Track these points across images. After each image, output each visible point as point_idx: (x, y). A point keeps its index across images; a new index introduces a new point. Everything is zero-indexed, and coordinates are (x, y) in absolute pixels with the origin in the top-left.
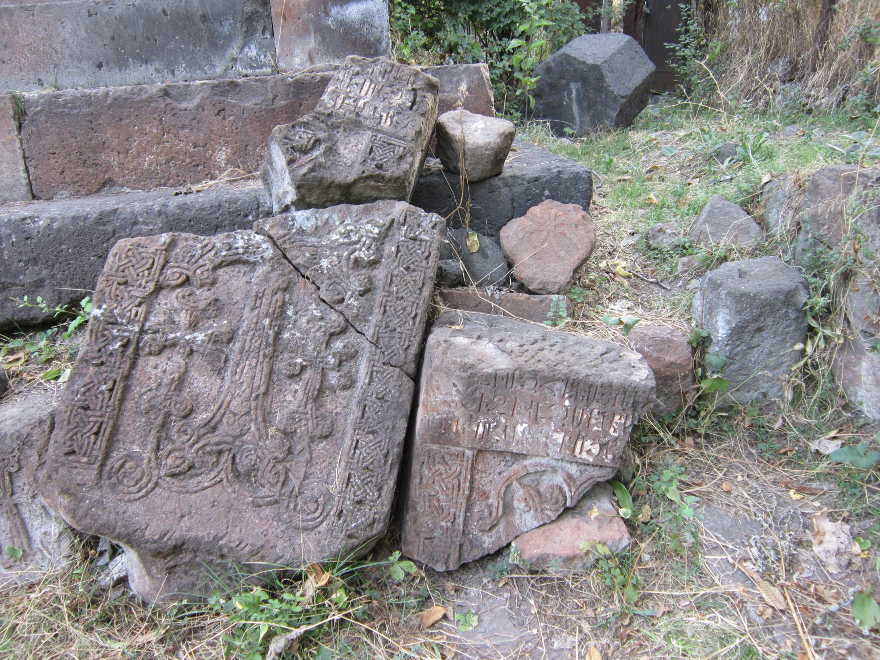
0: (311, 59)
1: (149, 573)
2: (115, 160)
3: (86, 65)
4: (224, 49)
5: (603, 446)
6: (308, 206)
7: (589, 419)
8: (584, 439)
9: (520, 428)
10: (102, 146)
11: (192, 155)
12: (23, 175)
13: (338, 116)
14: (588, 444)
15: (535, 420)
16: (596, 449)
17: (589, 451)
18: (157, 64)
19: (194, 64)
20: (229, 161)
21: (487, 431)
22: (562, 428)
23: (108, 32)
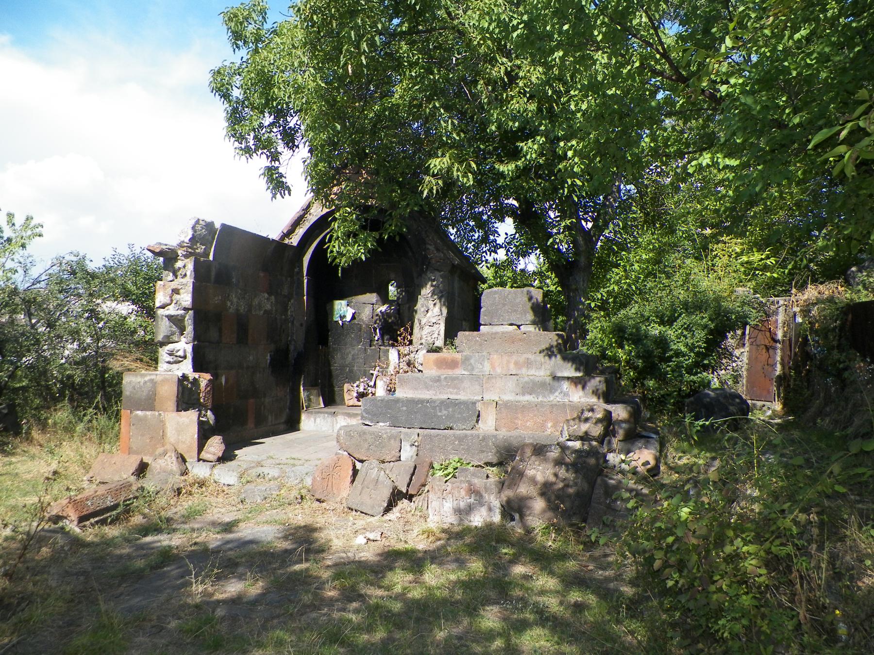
2: (520, 422)
3: (513, 394)
10: (517, 418)
19: (544, 396)
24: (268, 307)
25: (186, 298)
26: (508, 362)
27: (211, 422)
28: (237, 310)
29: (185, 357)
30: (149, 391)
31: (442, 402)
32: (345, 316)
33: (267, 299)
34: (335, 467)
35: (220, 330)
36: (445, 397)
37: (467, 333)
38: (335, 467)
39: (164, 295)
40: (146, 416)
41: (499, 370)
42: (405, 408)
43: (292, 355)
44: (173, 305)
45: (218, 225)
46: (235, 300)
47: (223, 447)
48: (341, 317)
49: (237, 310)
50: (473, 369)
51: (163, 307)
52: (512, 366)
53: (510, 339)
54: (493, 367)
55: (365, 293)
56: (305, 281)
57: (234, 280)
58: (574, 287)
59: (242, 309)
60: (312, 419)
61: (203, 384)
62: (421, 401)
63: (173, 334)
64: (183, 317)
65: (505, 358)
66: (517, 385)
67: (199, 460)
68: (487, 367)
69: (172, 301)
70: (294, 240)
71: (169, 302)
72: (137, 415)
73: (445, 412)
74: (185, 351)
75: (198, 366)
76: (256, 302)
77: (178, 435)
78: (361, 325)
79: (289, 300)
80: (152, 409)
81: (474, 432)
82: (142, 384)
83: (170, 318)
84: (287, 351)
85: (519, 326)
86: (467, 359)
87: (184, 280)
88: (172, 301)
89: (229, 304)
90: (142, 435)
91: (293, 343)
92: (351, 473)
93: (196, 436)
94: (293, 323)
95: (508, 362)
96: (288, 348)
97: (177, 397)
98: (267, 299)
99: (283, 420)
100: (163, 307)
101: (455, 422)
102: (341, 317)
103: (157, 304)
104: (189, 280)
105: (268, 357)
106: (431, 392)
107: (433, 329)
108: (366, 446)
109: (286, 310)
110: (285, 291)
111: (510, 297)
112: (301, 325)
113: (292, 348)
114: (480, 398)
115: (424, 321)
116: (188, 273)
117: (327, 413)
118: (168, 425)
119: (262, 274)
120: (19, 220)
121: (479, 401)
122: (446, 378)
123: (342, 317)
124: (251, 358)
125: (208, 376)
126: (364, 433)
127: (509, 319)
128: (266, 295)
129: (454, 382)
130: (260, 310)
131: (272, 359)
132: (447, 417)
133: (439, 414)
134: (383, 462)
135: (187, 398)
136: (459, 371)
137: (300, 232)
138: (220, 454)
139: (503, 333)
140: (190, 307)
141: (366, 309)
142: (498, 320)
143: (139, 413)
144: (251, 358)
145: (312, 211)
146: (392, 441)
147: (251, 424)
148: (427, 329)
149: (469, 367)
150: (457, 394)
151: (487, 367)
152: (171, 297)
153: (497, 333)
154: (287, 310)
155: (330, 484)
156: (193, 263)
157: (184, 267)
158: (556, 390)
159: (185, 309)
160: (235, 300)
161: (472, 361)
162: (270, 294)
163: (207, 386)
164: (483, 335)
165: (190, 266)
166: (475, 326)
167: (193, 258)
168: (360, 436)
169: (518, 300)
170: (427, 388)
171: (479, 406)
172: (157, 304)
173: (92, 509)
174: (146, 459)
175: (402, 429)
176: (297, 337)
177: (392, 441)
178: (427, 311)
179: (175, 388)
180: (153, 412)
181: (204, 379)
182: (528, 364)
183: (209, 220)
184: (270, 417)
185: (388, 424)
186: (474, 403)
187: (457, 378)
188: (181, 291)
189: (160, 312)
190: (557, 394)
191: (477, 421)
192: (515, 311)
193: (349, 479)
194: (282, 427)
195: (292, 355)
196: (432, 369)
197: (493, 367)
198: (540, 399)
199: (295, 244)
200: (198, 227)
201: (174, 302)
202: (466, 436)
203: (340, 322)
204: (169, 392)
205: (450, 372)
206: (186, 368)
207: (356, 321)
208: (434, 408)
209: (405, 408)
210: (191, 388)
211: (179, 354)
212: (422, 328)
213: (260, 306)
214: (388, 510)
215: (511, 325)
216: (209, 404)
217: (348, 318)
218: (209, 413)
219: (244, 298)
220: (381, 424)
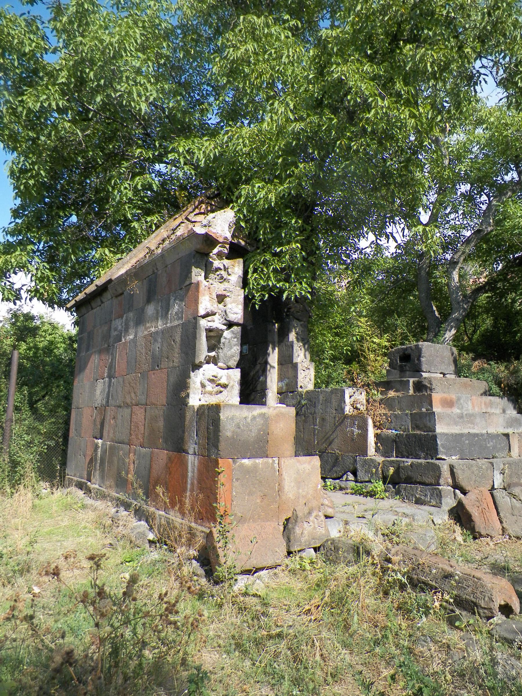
30: (259, 430)
36: (466, 431)
40: (255, 466)
51: (207, 315)
52: (483, 406)
54: (473, 407)
62: (462, 435)
72: (242, 465)
77: (299, 488)
82: (249, 420)
83: (209, 330)
86: (459, 399)
90: (250, 494)
101: (498, 452)
103: (202, 312)
106: (458, 427)
118: (285, 475)
126: (472, 466)
143: (246, 462)
161: (462, 401)
170: (456, 423)
179: (294, 426)
180: (265, 460)
185: (458, 457)
211: (223, 381)
220: (454, 457)
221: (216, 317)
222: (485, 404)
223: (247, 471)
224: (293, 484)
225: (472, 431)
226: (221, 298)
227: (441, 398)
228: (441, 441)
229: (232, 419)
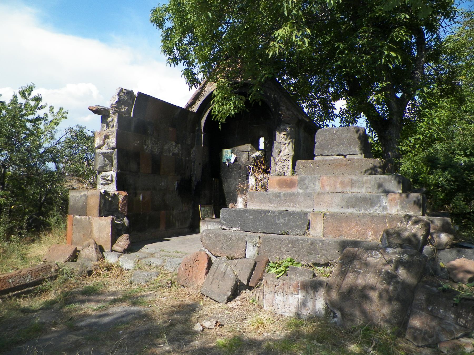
0: (398, 211)
1: (343, 320)
2: (344, 230)
3: (339, 207)
4: (374, 206)
5: (466, 322)
6: (391, 248)
7: (462, 313)
8: (460, 318)
9: (441, 311)
10: (341, 227)
11: (363, 232)
12: (322, 230)
13: (401, 228)
14: (461, 319)
15: (445, 310)
16: (464, 322)
17: (462, 322)
18: (356, 209)
19: (365, 209)
20: (372, 235)
21: (432, 309)
22: (454, 314)
23: (346, 200)
24: (176, 151)
25: (113, 141)
26: (335, 182)
27: (126, 225)
28: (152, 151)
29: (112, 181)
30: (84, 202)
31: (280, 212)
32: (230, 160)
33: (175, 146)
34: (195, 260)
35: (139, 164)
36: (283, 209)
37: (303, 161)
38: (195, 260)
39: (100, 140)
40: (81, 219)
41: (327, 189)
42: (251, 217)
43: (194, 184)
44: (105, 146)
45: (136, 93)
46: (150, 145)
47: (128, 242)
48: (227, 160)
49: (152, 151)
50: (307, 188)
51: (99, 147)
52: (338, 185)
53: (338, 165)
54: (323, 186)
55: (244, 144)
56: (203, 135)
57: (149, 131)
58: (389, 138)
59: (156, 151)
60: (206, 226)
61: (121, 198)
62: (264, 212)
63: (106, 165)
64: (112, 153)
65: (333, 179)
66: (343, 199)
67: (112, 251)
68: (318, 186)
69: (104, 143)
70: (195, 109)
71: (102, 144)
73: (282, 221)
74: (112, 177)
75: (119, 188)
76: (166, 147)
78: (241, 166)
79: (192, 148)
80: (85, 215)
81: (305, 237)
82: (79, 197)
83: (104, 154)
84: (190, 180)
85: (345, 156)
86: (302, 180)
87: (112, 130)
88: (104, 143)
89: (145, 147)
91: (194, 176)
92: (206, 266)
93: (110, 234)
94: (194, 162)
95: (335, 182)
96: (191, 178)
97: (100, 206)
98: (175, 146)
99: (187, 226)
100: (99, 147)
101: (290, 229)
102: (227, 160)
103: (96, 146)
104: (115, 129)
105: (176, 184)
106: (273, 205)
107: (284, 164)
108: (220, 245)
109: (189, 154)
110: (189, 142)
111: (338, 133)
112: (200, 164)
113: (194, 179)
114: (311, 210)
115: (277, 159)
116: (115, 125)
117: (215, 222)
118: (94, 225)
119: (171, 129)
120: (56, 110)
121: (310, 212)
122: (285, 194)
123: (229, 160)
124: (163, 184)
125: (124, 193)
126: (219, 235)
127: (337, 151)
128: (174, 143)
129: (291, 198)
130: (170, 153)
131: (179, 185)
132: (284, 224)
133: (278, 222)
134: (232, 258)
135: (107, 206)
136: (296, 190)
137: (199, 103)
138: (126, 247)
139: (331, 160)
140: (115, 147)
141: (244, 155)
142: (329, 151)
143: (77, 217)
144: (163, 184)
145: (206, 89)
146: (240, 242)
147: (162, 227)
148: (280, 165)
149: (304, 187)
150: (293, 206)
151: (318, 186)
152: (104, 141)
153: (327, 160)
154: (190, 154)
155: (191, 273)
156: (117, 118)
157: (112, 120)
158: (376, 204)
159: (113, 148)
160: (150, 145)
161: (306, 182)
162: (177, 143)
163: (123, 200)
164: (316, 162)
165: (116, 120)
166: (312, 157)
167: (117, 114)
168: (216, 237)
169: (344, 136)
170: (270, 202)
171: (310, 217)
172: (96, 146)
173: (12, 285)
174: (79, 248)
175: (249, 233)
176: (197, 173)
177: (240, 242)
178: (280, 152)
179: (99, 201)
181: (122, 195)
182: (352, 183)
183: (129, 89)
184: (177, 224)
185: (239, 229)
186: (306, 214)
187: (293, 194)
188: (110, 136)
189: (98, 151)
190: (377, 207)
191: (308, 229)
192: (342, 144)
193: (204, 271)
194: (186, 230)
195: (194, 184)
196: (275, 188)
197: (323, 186)
198: (362, 211)
199: (195, 111)
200: (122, 94)
201: (106, 144)
202: (298, 240)
203: (227, 163)
204: (94, 202)
205: (289, 191)
206: (112, 189)
207: (237, 163)
208: (274, 217)
209: (251, 217)
210: (111, 201)
212: (276, 164)
213: (169, 150)
214: (230, 299)
215: (339, 155)
216: (125, 212)
217: (232, 161)
218: (125, 219)
219: (158, 144)
220: (234, 229)
221: (104, 147)
222: (342, 183)
223: (79, 221)
224: (97, 231)
225: (289, 209)
226: (107, 137)
227: (279, 180)
228: (222, 214)
229: (73, 197)
